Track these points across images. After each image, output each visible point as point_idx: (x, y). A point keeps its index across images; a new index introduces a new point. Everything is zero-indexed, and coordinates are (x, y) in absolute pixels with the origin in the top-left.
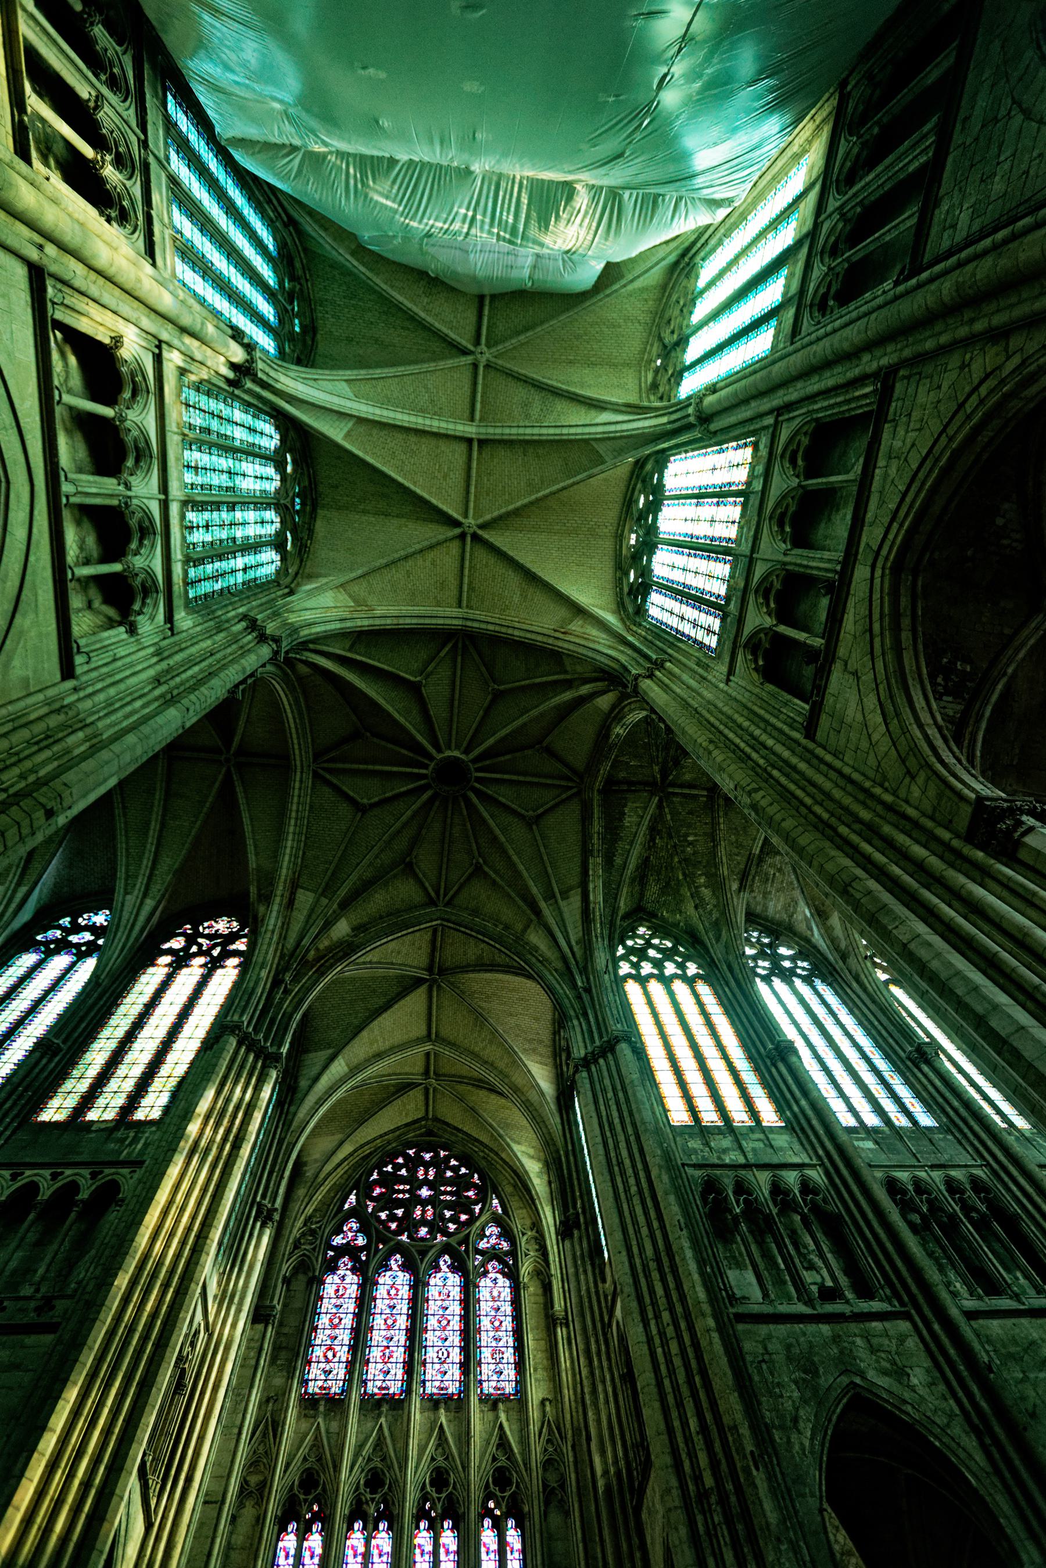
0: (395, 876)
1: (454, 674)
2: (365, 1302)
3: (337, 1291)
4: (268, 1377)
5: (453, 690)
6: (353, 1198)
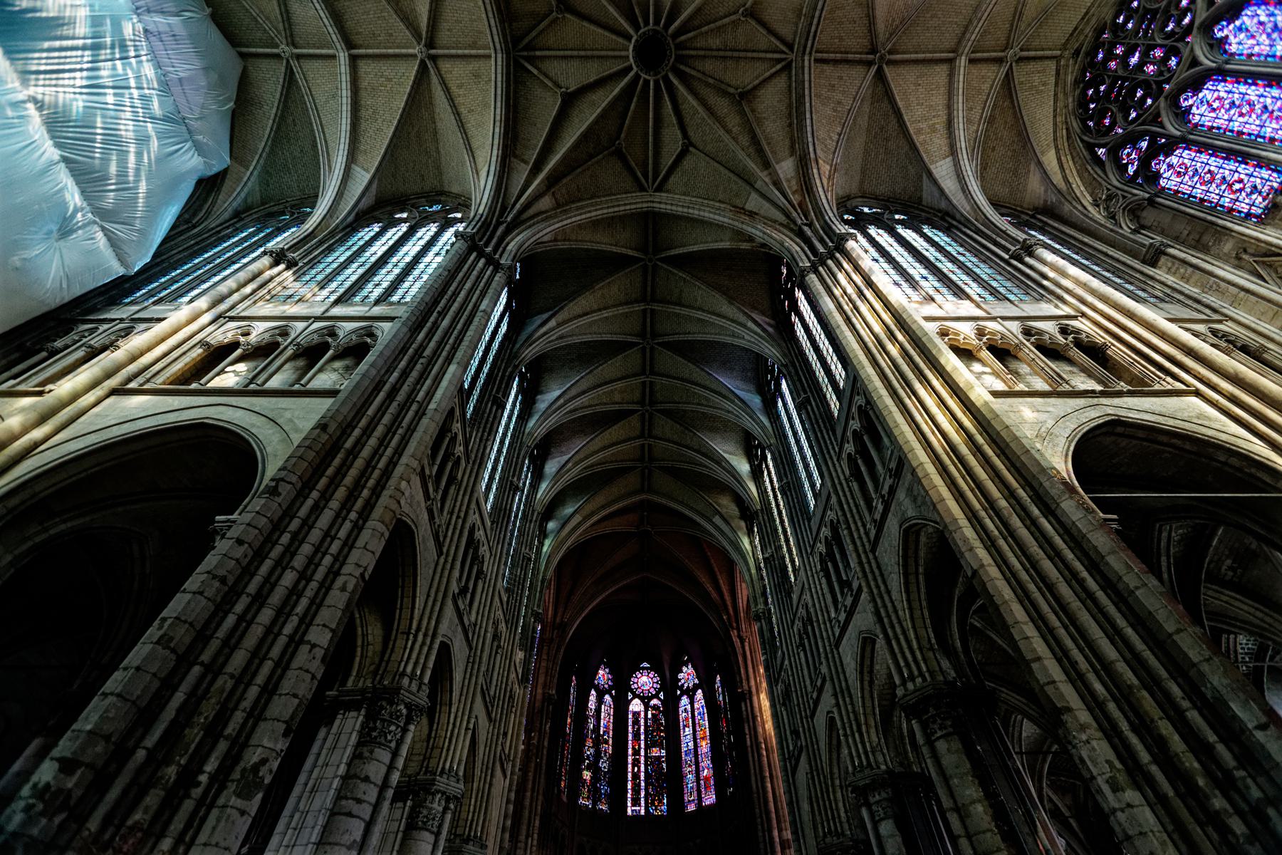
0: (753, 111)
1: (556, 57)
2: (1206, 142)
3: (1179, 174)
4: (1218, 257)
5: (572, 57)
6: (1101, 151)
